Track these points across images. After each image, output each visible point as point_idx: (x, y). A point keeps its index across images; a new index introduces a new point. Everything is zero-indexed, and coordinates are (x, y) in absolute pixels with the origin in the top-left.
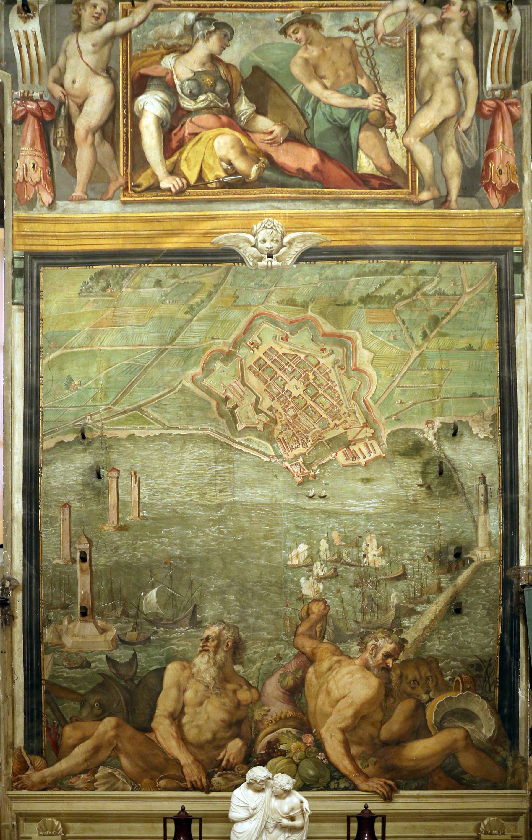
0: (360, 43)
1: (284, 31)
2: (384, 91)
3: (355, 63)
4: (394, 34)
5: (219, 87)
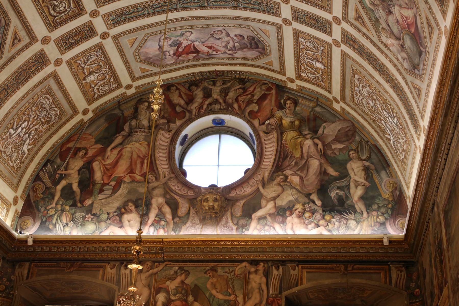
0: (230, 277)
1: (206, 273)
2: (236, 294)
3: (227, 284)
4: (241, 274)
5: (183, 292)
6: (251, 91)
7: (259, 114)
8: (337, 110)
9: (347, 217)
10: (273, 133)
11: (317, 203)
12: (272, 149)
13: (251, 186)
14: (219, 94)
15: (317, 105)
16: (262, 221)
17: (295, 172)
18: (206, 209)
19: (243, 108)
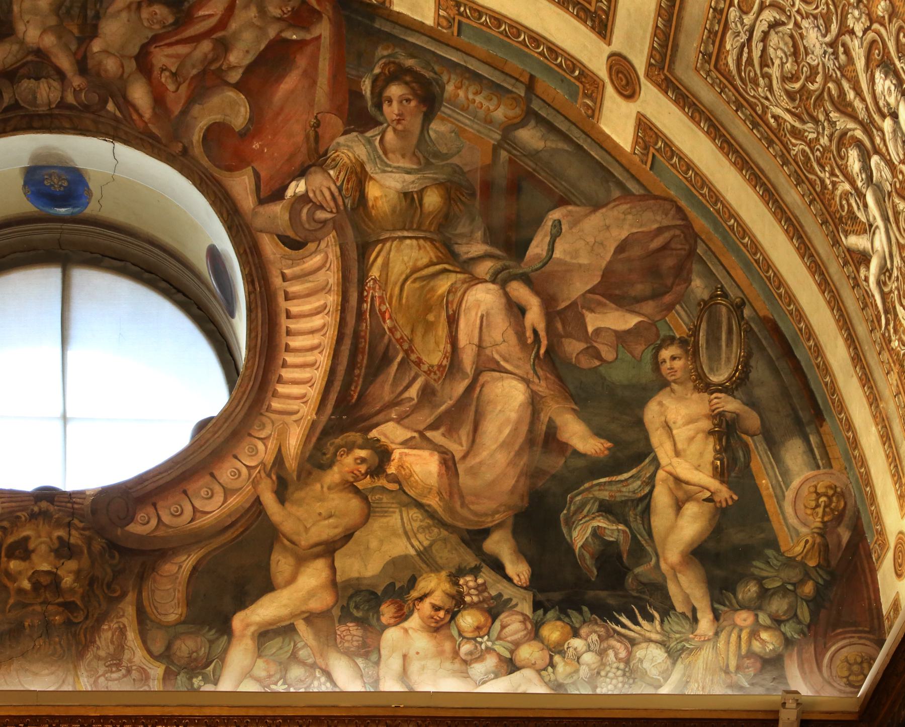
6: (212, 22)
7: (256, 146)
8: (616, 146)
9: (634, 631)
10: (323, 245)
11: (510, 570)
12: (317, 321)
13: (228, 492)
14: (52, 21)
15: (530, 116)
16: (274, 645)
17: (421, 434)
18: (21, 591)
19: (177, 110)
